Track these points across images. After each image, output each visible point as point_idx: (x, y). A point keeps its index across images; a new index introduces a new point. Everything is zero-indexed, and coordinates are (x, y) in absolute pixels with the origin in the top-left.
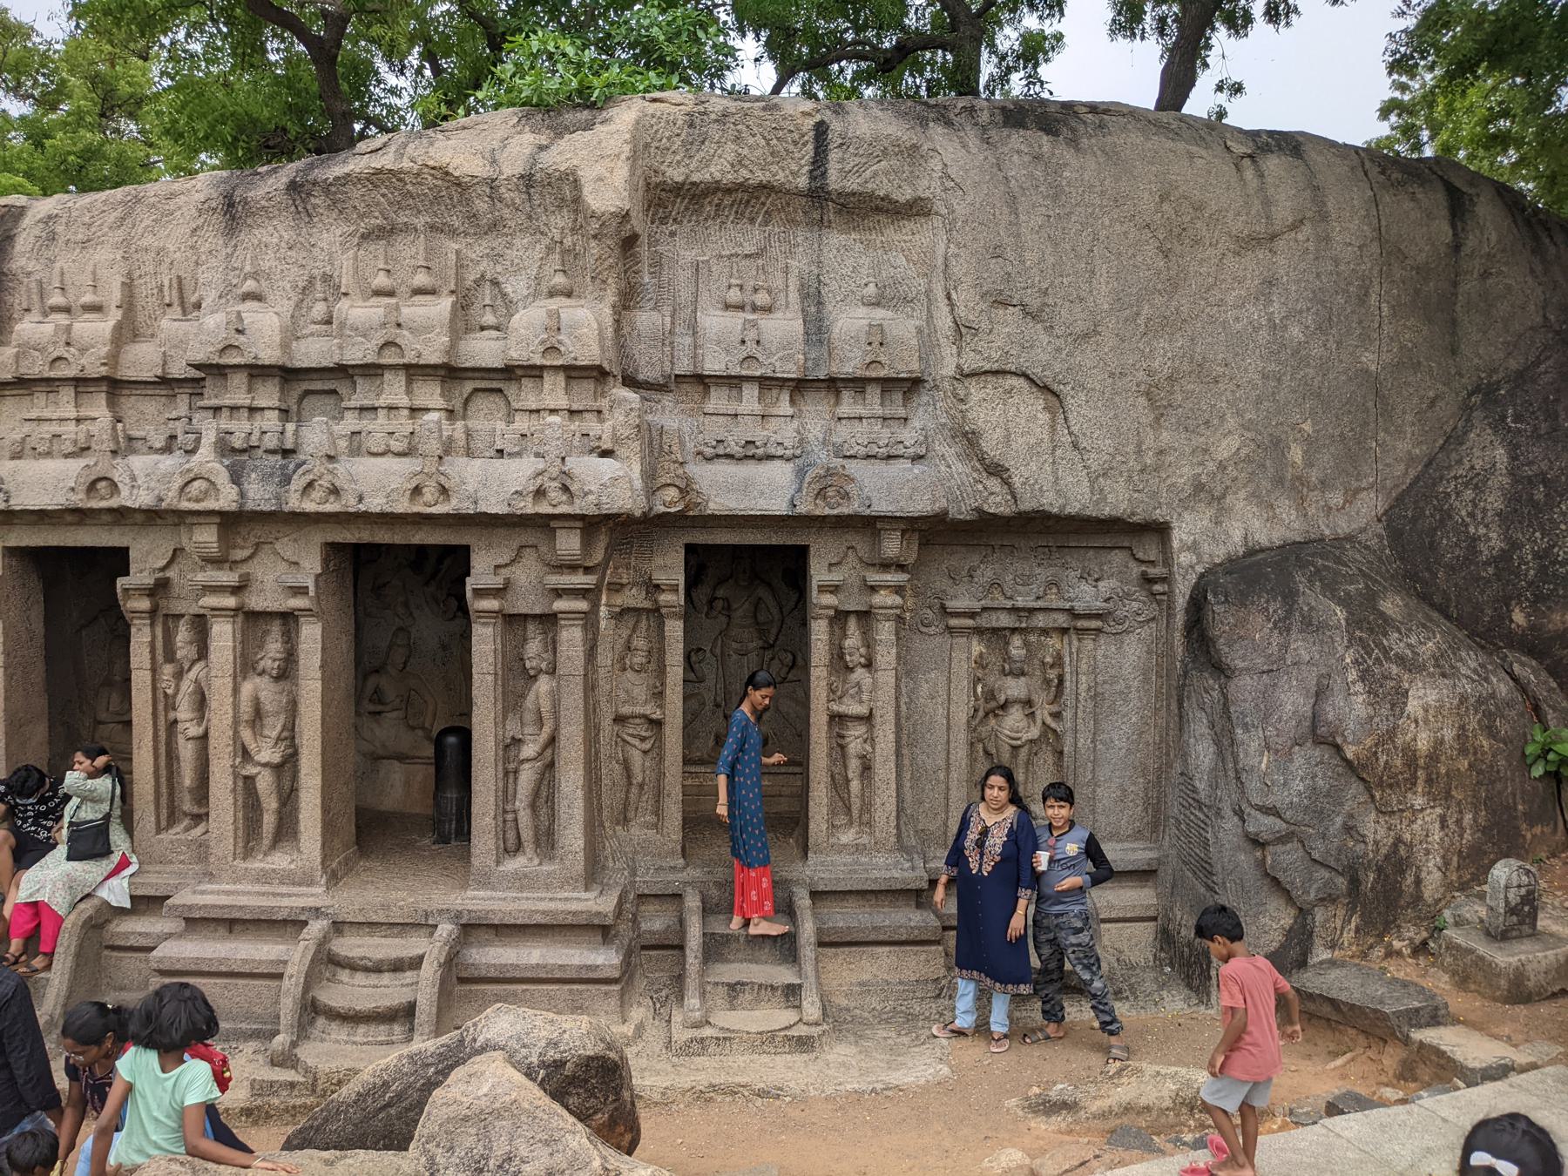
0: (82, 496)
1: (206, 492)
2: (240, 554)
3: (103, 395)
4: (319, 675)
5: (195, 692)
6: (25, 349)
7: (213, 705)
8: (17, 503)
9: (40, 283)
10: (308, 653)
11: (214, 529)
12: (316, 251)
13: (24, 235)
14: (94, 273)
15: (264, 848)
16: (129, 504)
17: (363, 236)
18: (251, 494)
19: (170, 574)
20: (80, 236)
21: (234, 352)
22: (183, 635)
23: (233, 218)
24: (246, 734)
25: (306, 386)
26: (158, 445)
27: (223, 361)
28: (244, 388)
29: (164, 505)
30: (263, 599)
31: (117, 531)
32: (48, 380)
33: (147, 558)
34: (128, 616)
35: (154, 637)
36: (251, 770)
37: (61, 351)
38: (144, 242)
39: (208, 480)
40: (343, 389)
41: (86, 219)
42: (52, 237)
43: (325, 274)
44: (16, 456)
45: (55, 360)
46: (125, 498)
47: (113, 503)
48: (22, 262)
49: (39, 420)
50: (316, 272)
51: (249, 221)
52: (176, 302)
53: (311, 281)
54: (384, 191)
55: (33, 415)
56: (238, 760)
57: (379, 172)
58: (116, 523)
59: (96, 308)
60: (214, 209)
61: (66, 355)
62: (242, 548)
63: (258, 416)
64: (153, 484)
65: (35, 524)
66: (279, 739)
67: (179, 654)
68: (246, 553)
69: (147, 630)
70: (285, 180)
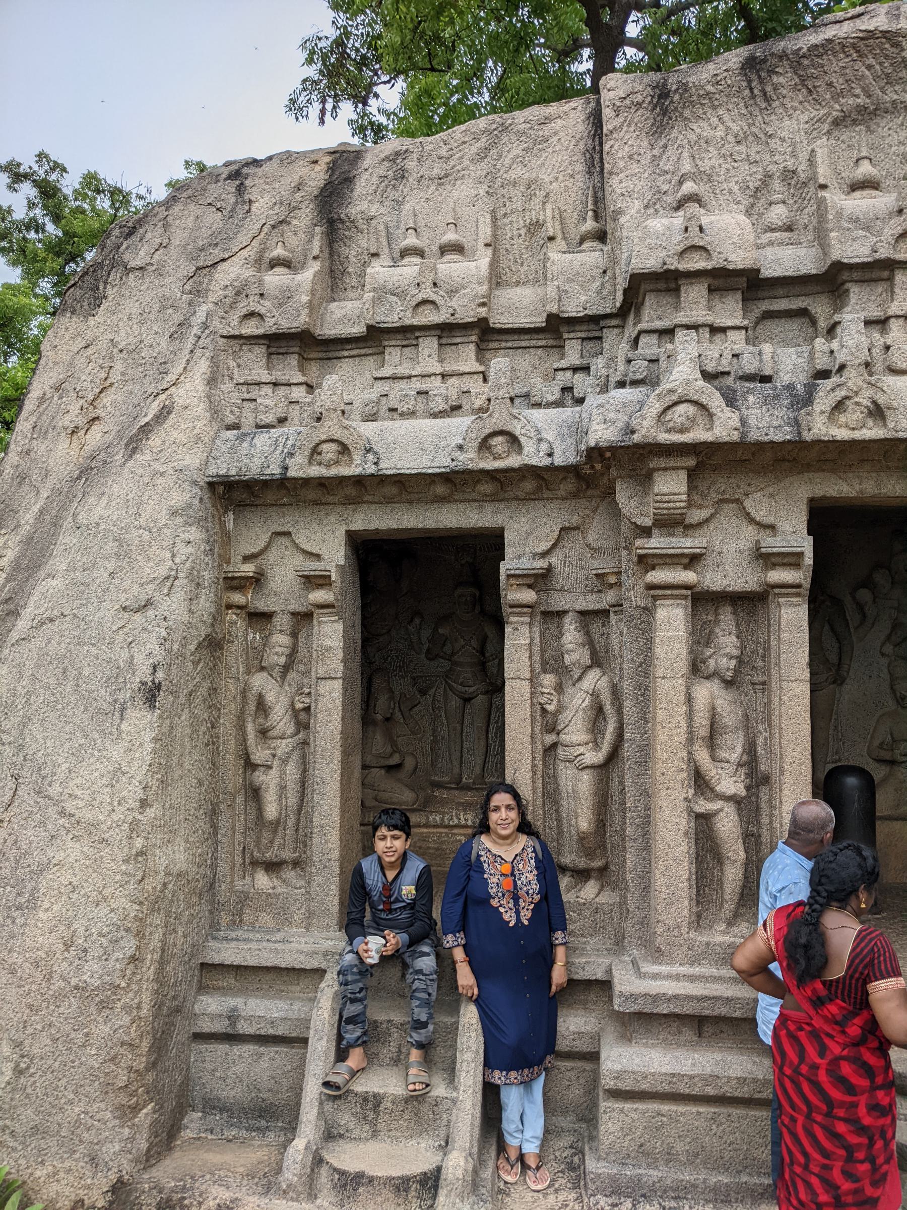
0: (472, 454)
1: (693, 420)
2: (696, 515)
3: (472, 347)
4: (806, 674)
5: (591, 707)
6: (383, 293)
7: (661, 715)
8: (389, 466)
9: (387, 228)
10: (790, 644)
11: (683, 476)
12: (774, 143)
13: (366, 176)
14: (454, 210)
15: (729, 915)
16: (535, 462)
17: (836, 123)
18: (752, 421)
19: (555, 560)
20: (436, 171)
21: (696, 255)
22: (571, 635)
23: (664, 112)
24: (703, 756)
25: (765, 306)
26: (551, 398)
27: (683, 266)
28: (703, 301)
29: (636, 438)
30: (730, 572)
31: (489, 508)
32: (407, 334)
33: (527, 539)
34: (506, 610)
35: (532, 640)
36: (704, 806)
37: (427, 293)
38: (512, 175)
39: (696, 403)
40: (820, 308)
41: (444, 152)
42: (402, 175)
43: (785, 170)
44: (372, 417)
45: (418, 305)
46: (532, 455)
47: (513, 461)
48: (363, 206)
49: (395, 378)
50: (772, 168)
51: (687, 113)
52: (559, 236)
53: (768, 176)
54: (871, 61)
55: (387, 371)
56: (691, 792)
57: (870, 34)
58: (493, 498)
59: (457, 248)
60: (639, 104)
61: (434, 297)
62: (700, 507)
63: (718, 338)
64: (612, 415)
65: (389, 501)
66: (740, 765)
67: (568, 659)
68: (704, 514)
69: (525, 630)
70: (746, 54)
